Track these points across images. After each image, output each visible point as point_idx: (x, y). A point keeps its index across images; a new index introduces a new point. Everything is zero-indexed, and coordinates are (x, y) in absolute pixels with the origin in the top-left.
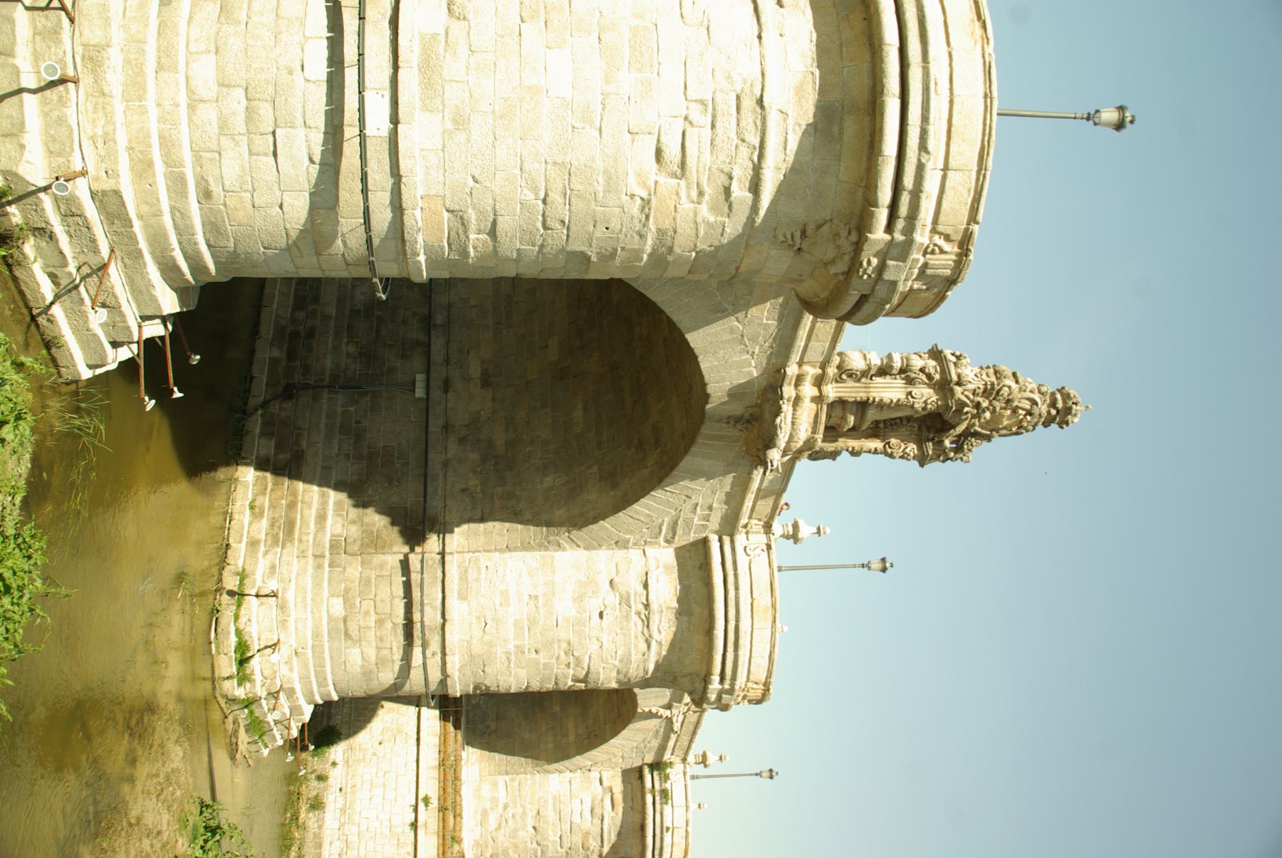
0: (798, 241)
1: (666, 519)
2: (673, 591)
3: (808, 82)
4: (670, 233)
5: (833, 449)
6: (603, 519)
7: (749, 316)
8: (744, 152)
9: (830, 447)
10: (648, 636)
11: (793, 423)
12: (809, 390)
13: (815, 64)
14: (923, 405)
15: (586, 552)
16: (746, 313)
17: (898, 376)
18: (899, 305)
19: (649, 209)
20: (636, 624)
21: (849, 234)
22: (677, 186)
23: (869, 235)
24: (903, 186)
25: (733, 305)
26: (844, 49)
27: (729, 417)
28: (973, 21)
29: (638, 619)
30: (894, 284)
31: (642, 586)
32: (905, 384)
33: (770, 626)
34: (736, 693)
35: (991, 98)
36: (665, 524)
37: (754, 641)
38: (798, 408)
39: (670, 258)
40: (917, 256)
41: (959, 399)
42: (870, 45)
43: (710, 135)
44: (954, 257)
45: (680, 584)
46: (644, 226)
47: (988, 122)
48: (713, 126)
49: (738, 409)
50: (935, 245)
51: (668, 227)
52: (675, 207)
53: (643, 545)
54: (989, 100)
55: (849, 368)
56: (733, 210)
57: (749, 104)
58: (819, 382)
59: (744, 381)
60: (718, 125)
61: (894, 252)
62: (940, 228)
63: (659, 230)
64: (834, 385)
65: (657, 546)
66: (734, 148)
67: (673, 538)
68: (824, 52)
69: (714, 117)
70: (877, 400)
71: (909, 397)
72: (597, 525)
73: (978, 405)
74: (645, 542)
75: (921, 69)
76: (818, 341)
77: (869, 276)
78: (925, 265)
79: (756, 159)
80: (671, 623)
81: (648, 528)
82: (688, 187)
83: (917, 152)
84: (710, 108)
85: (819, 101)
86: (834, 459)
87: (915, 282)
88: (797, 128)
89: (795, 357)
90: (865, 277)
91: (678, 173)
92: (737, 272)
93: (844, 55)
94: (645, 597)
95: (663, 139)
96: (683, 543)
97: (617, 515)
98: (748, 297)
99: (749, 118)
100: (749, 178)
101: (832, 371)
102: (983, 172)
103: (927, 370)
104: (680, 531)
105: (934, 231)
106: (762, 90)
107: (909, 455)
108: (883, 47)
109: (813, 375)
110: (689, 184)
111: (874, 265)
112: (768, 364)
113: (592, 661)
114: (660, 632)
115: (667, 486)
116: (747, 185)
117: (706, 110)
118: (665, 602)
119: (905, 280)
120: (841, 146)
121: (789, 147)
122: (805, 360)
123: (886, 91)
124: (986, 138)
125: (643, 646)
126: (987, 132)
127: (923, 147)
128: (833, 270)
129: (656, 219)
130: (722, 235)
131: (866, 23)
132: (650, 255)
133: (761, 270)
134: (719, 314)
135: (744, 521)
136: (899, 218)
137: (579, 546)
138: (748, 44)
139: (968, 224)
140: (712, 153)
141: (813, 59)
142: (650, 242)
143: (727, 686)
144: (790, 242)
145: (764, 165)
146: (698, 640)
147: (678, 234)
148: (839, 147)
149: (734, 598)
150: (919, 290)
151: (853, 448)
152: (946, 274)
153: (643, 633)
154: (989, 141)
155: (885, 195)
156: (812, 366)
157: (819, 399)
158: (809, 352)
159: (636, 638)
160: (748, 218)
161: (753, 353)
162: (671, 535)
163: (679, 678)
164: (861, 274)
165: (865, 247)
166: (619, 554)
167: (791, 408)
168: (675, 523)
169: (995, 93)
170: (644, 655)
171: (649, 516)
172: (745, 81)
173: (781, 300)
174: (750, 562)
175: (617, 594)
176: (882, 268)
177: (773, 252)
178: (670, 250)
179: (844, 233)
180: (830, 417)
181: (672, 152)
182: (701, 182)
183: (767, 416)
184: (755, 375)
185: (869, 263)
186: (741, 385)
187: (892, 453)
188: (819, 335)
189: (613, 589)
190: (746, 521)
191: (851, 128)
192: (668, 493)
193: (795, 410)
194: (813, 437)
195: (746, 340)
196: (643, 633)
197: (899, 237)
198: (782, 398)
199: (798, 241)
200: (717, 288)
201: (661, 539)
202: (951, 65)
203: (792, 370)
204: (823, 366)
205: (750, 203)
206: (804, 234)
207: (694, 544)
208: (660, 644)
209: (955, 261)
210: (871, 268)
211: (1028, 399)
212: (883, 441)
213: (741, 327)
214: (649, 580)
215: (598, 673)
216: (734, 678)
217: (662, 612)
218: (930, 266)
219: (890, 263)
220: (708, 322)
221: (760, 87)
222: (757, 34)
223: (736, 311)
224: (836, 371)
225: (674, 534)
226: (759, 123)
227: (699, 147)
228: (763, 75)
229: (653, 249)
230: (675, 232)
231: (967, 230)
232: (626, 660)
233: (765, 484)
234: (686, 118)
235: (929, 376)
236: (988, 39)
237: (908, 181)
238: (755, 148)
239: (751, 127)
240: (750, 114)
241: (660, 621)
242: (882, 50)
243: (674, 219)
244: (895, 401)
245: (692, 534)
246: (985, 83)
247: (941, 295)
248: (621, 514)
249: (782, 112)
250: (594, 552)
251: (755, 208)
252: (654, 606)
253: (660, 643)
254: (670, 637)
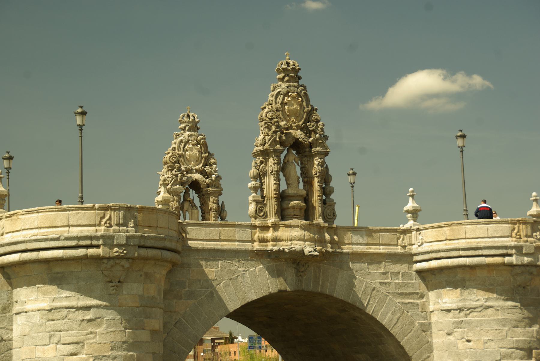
0: (114, 284)
1: (398, 301)
2: (451, 292)
3: (41, 289)
4: (114, 344)
5: (320, 208)
6: (400, 342)
7: (215, 278)
8: (71, 315)
9: (318, 211)
10: (482, 308)
11: (291, 240)
12: (269, 234)
13: (34, 287)
14: (276, 165)
15: (434, 352)
16: (214, 280)
17: (263, 181)
18: (150, 227)
19: (100, 356)
20: (474, 317)
21: (104, 263)
22: (88, 345)
23: (101, 256)
24: (76, 245)
25: (208, 289)
26: (28, 274)
27: (296, 275)
28: (11, 220)
29: (470, 315)
30: (128, 237)
31: (449, 313)
32: (267, 177)
33: (464, 227)
34: (522, 243)
35: (38, 210)
36: (403, 301)
37: (475, 236)
38: (281, 239)
39: (131, 341)
40: (111, 232)
41: (269, 145)
42: (24, 264)
43: (64, 332)
44: (113, 212)
45: (446, 288)
46: (109, 357)
47: (48, 210)
48: (60, 331)
49: (290, 272)
50: (106, 223)
51: (110, 346)
52: (98, 344)
53: (426, 313)
54: (39, 211)
55: (254, 213)
56: (99, 316)
57: (51, 316)
58: (264, 228)
59: (267, 272)
60: (59, 329)
61: (109, 242)
62: (97, 222)
63: (111, 350)
64: (268, 218)
65: (426, 304)
66: (69, 321)
67: (417, 294)
68: (30, 284)
69: (56, 331)
70: (275, 192)
71: (272, 173)
72: (404, 346)
73: (275, 132)
74: (422, 312)
75: (28, 244)
76: (234, 235)
77: (124, 250)
78: (118, 225)
79: (74, 310)
80: (472, 293)
81: (408, 312)
82: (88, 339)
83: (60, 241)
84: (52, 333)
85: (48, 284)
86: (335, 203)
87: (129, 225)
88: (60, 292)
89: (248, 246)
90: (125, 252)
91: (82, 345)
92: (141, 306)
93: (30, 274)
94: (455, 311)
95: (65, 354)
96: (423, 286)
97: (394, 334)
98: (202, 281)
99: (57, 315)
100: (83, 311)
101: (257, 222)
102: (69, 209)
103: (259, 164)
104: (411, 290)
105: (99, 225)
106: (45, 310)
107: (319, 162)
108: (21, 260)
109: (260, 233)
110: (86, 339)
111: (118, 249)
112: (252, 260)
113: (505, 346)
114: (478, 300)
115: (363, 305)
116: (86, 312)
117: (54, 335)
118: (457, 297)
119: (127, 231)
120: (66, 272)
121: (68, 295)
122: (250, 239)
123: (37, 258)
124: (54, 210)
125: (490, 311)
126: (52, 210)
127: (58, 239)
129: (105, 352)
130: (114, 319)
131: (17, 266)
132: (128, 351)
133: (139, 296)
134: (215, 295)
135: (399, 250)
136: (92, 243)
137: (429, 357)
138: (29, 317)
139: (95, 209)
140: (72, 330)
141: (33, 288)
142: (119, 353)
143: (514, 251)
144: (115, 287)
145: (76, 306)
146: (481, 274)
147: (114, 340)
148: (66, 273)
149: (445, 253)
150: (134, 223)
151: (318, 196)
152: (123, 213)
153: (480, 312)
154: (56, 209)
155: (81, 252)
156: (255, 234)
157: (275, 227)
158: (244, 238)
159: (484, 316)
160: (104, 309)
161: (244, 271)
162: (415, 296)
163: (518, 283)
164: (123, 254)
165: (108, 256)
166: (434, 329)
167: (282, 243)
168: (401, 294)
169: (36, 208)
170: (498, 310)
171: (394, 313)
172: (42, 318)
173: (203, 263)
174: (426, 242)
175: (455, 330)
176: (119, 246)
177: (124, 292)
178: (124, 342)
179: (104, 265)
180: (295, 215)
181: (71, 349)
182: (86, 334)
183: (287, 256)
184: (262, 266)
185: (116, 252)
186: (270, 273)
187: (319, 172)
188: (230, 236)
189: (452, 333)
190: (399, 247)
191: (57, 269)
192: (371, 302)
193: (283, 240)
194: (300, 226)
195: (234, 277)
196: (480, 312)
197: (101, 242)
198: (272, 250)
199: (114, 284)
200: (196, 299)
201: (419, 301)
202: (27, 229)
203: (256, 246)
204: (253, 227)
205: (96, 309)
206: (111, 282)
207: (423, 279)
208: (487, 300)
209: (115, 211)
210: (119, 251)
211: (276, 98)
212: (314, 177)
213: (224, 282)
214: (445, 309)
215: (517, 341)
216: (506, 247)
217: (464, 299)
218: (118, 223)
219: (115, 243)
220: (221, 300)
221: (44, 311)
222: (25, 314)
223: (212, 286)
224: (257, 220)
225: (413, 293)
226: (58, 310)
227: (69, 337)
228: (39, 310)
229: (124, 350)
230: (113, 342)
231: (98, 210)
232: (503, 322)
233: (361, 240)
234: (57, 344)
235: (262, 162)
236: (17, 213)
237: (73, 243)
238: (69, 311)
239: (60, 314)
240: (55, 315)
241: (470, 300)
242: (22, 261)
243: (105, 343)
244: (275, 182)
245: (414, 281)
246: (33, 213)
247: (140, 209)
248: (392, 332)
249: (53, 300)
250: (435, 346)
251: (98, 307)
252: (460, 305)
253: (487, 299)
254: (481, 292)
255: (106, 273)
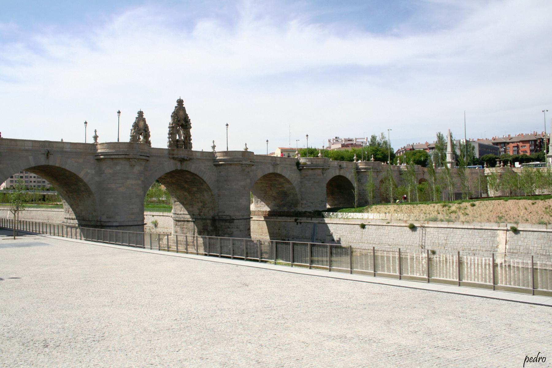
128: (136, 161)
255: (130, 163)
